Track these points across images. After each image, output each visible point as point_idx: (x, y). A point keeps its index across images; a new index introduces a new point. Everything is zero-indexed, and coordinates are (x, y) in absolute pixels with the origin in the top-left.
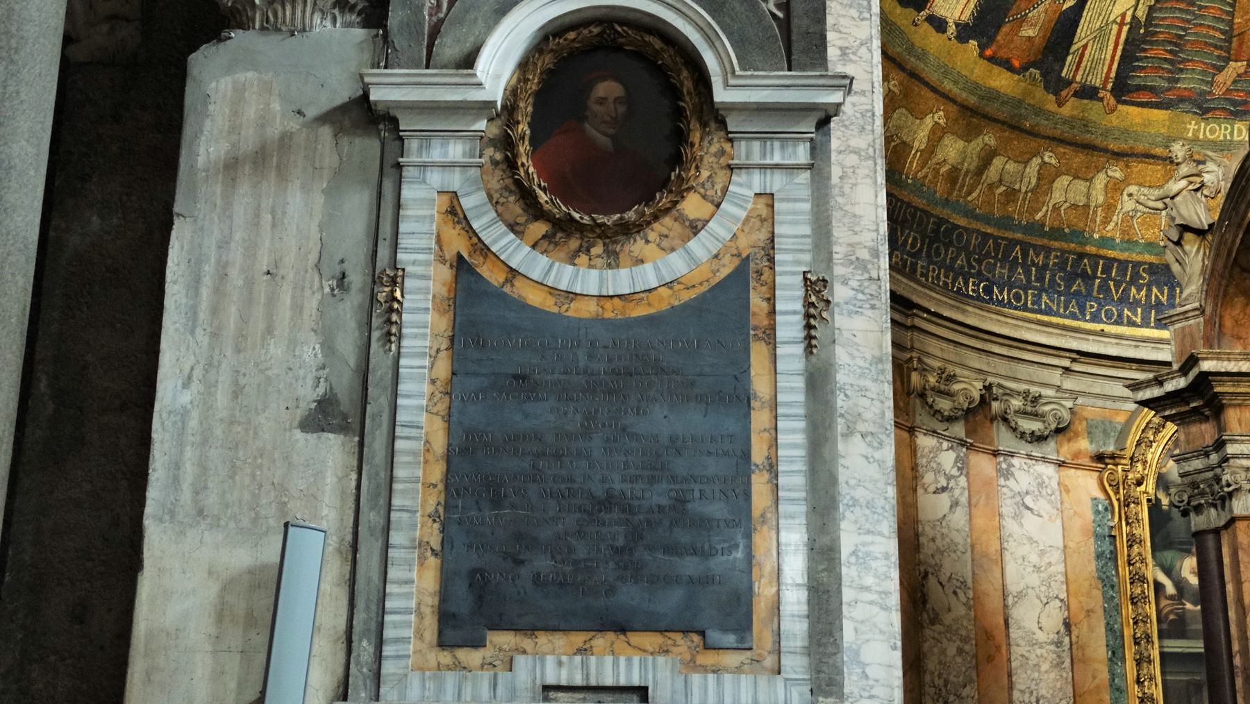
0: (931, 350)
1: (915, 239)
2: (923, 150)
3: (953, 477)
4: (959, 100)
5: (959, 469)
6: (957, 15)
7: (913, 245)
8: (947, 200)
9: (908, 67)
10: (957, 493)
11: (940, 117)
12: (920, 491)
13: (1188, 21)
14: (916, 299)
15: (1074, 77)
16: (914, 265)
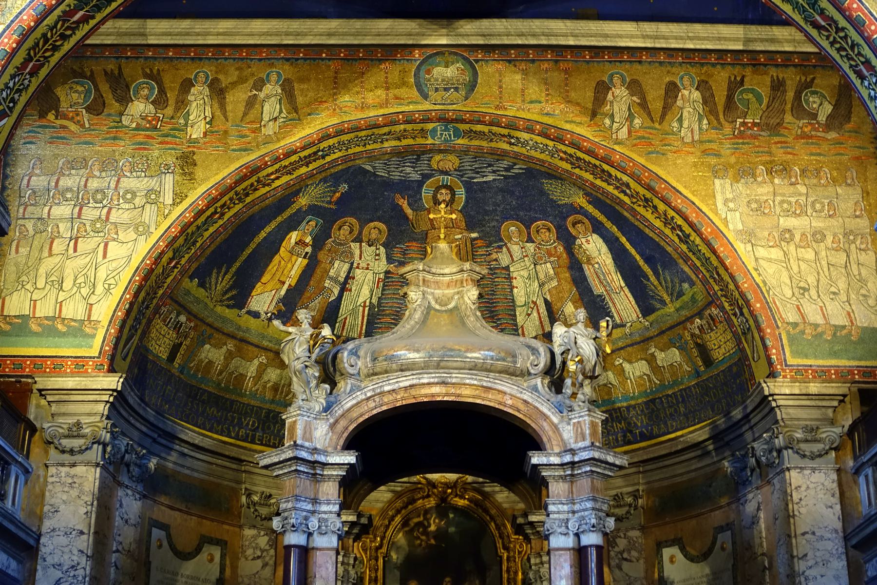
0: (257, 482)
1: (254, 422)
2: (254, 377)
3: (266, 550)
4: (273, 349)
5: (270, 545)
6: (265, 309)
7: (253, 425)
8: (273, 400)
9: (238, 337)
10: (267, 559)
11: (263, 359)
12: (243, 559)
13: (402, 304)
14: (243, 458)
15: (342, 333)
16: (254, 437)
